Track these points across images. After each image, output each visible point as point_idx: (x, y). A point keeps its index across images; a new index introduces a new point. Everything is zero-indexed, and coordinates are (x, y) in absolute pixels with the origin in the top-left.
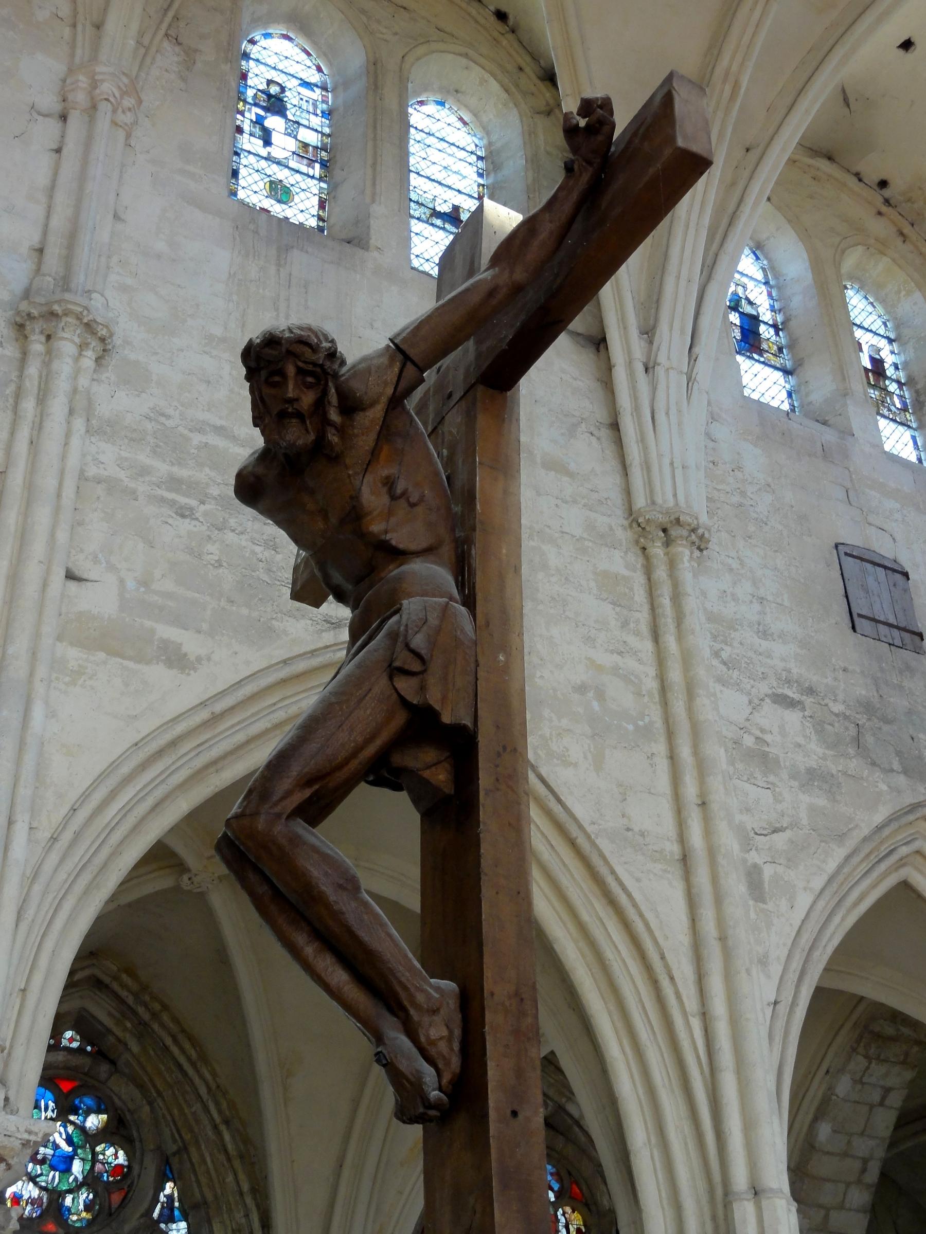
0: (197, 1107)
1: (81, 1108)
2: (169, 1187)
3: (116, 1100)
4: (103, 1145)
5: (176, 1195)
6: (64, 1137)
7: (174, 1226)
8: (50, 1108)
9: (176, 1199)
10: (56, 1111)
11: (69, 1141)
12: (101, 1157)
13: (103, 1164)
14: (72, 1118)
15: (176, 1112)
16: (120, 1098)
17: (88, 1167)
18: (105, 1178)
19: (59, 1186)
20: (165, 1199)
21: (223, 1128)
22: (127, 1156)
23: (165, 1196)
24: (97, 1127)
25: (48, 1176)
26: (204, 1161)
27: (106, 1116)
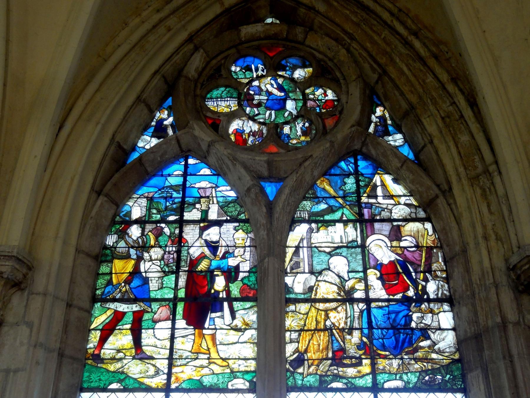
0: (386, 33)
1: (287, 66)
2: (379, 111)
3: (317, 54)
4: (312, 89)
5: (387, 115)
6: (275, 86)
7: (390, 138)
8: (260, 69)
9: (388, 118)
10: (265, 71)
11: (280, 88)
12: (311, 96)
13: (314, 101)
14: (280, 73)
15: (368, 45)
16: (320, 52)
17: (300, 104)
18: (318, 111)
19: (276, 120)
20: (378, 120)
21: (411, 38)
22: (335, 94)
23: (377, 117)
24: (305, 77)
25: (265, 115)
26: (403, 73)
27: (310, 70)
